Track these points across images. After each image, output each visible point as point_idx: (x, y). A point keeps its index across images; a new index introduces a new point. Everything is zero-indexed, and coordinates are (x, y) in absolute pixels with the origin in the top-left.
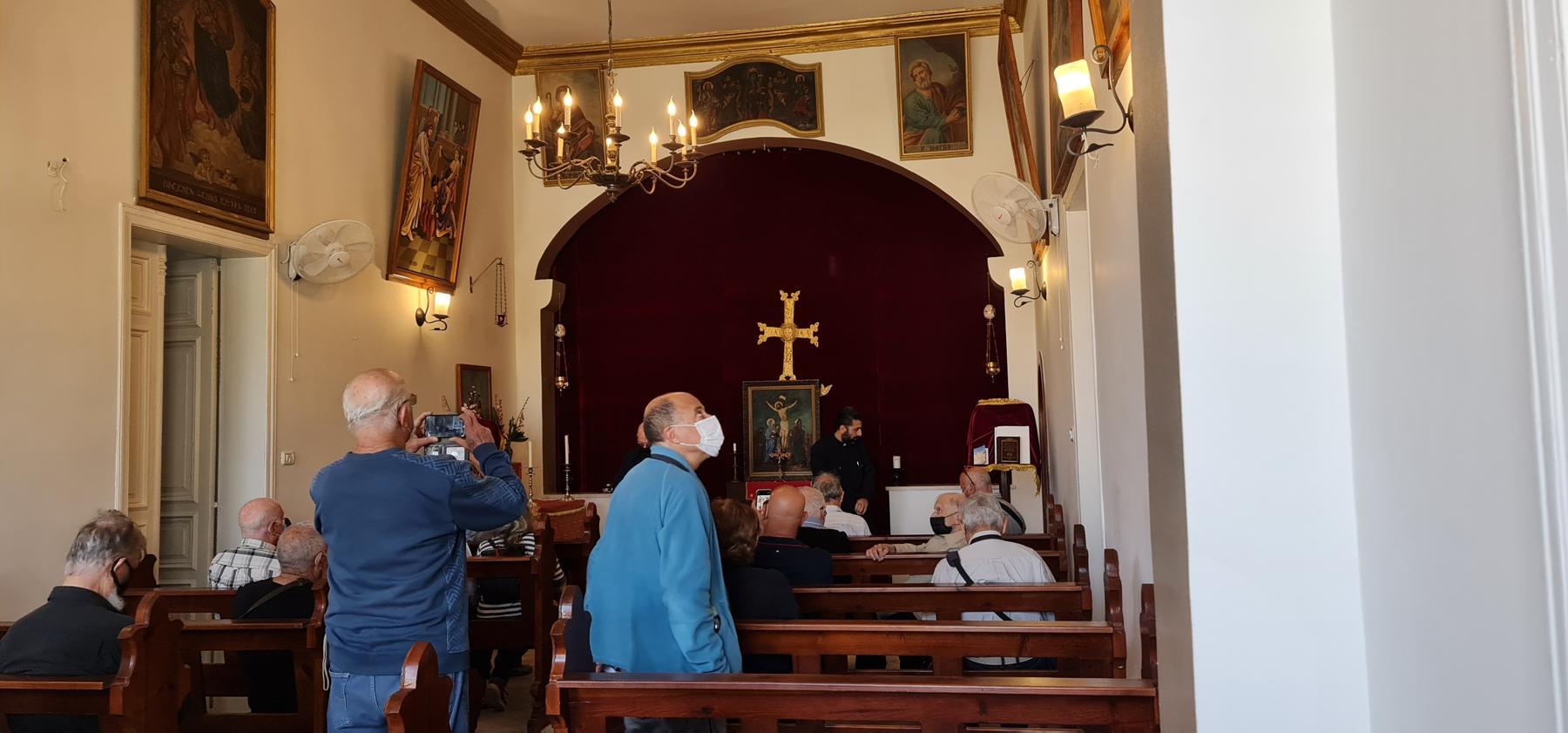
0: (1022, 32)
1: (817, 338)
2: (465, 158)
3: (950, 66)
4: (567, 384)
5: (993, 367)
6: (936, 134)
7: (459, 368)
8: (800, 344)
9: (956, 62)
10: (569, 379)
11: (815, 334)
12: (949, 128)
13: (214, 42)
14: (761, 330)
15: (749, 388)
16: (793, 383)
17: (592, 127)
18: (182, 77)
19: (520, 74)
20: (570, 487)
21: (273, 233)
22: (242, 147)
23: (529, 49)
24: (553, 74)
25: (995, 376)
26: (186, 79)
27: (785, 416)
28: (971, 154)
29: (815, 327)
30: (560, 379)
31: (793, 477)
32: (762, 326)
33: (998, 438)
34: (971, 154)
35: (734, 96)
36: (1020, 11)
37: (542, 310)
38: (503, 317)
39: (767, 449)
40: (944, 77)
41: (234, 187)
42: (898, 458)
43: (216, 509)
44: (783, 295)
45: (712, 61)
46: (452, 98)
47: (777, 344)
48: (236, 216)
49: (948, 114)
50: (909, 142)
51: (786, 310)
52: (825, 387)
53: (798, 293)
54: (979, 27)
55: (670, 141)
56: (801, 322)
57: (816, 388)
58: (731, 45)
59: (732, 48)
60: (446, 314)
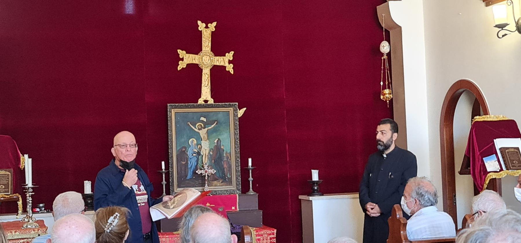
1: (232, 65)
14: (181, 57)
15: (172, 110)
16: (211, 106)
25: (389, 101)
27: (206, 136)
29: (230, 56)
31: (215, 191)
32: (182, 53)
39: (189, 167)
44: (201, 26)
53: (215, 24)
57: (234, 110)
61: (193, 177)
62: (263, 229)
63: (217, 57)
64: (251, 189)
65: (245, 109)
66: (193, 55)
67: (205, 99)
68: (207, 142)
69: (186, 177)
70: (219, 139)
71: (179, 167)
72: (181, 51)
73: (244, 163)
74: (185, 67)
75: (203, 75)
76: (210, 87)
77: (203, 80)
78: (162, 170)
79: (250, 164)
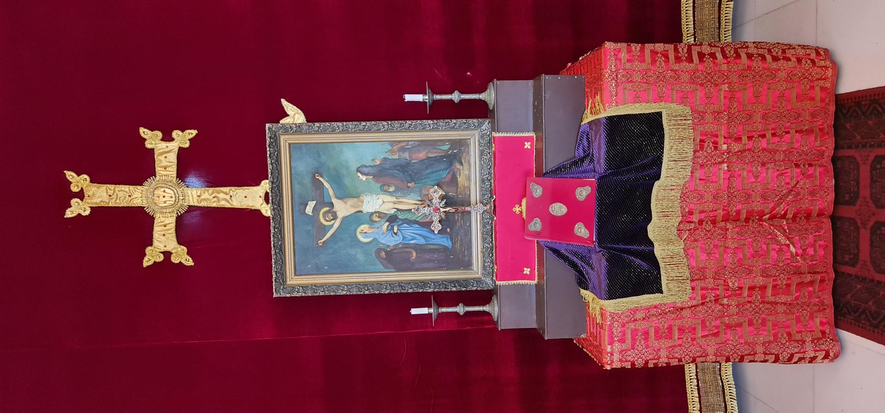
1: (176, 134)
11: (167, 138)
14: (161, 258)
15: (289, 282)
27: (351, 202)
29: (151, 138)
32: (151, 257)
39: (422, 241)
44: (77, 209)
52: (287, 115)
53: (70, 175)
61: (447, 232)
63: (158, 169)
65: (283, 101)
67: (261, 201)
68: (366, 199)
69: (446, 249)
70: (358, 170)
71: (426, 265)
72: (146, 259)
73: (417, 112)
74: (185, 248)
76: (233, 188)
77: (214, 205)
79: (419, 98)
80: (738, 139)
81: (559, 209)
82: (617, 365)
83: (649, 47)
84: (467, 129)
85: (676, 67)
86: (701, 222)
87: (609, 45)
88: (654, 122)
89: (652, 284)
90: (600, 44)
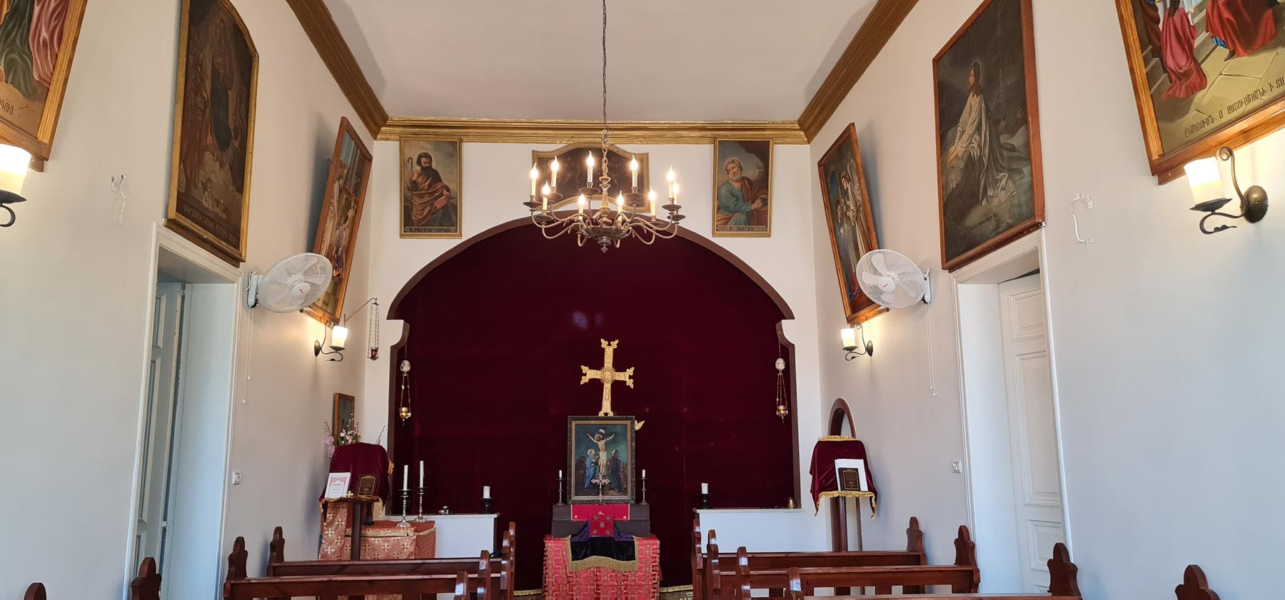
0: (809, 143)
2: (357, 208)
3: (757, 165)
4: (409, 414)
5: (783, 410)
6: (743, 217)
7: (337, 396)
8: (618, 386)
9: (763, 163)
10: (411, 410)
11: (630, 377)
12: (753, 213)
13: (222, 81)
16: (611, 419)
17: (448, 190)
18: (201, 110)
19: (382, 139)
20: (423, 509)
21: (245, 262)
22: (231, 180)
23: (394, 119)
24: (416, 142)
26: (204, 112)
27: (604, 447)
28: (769, 236)
29: (630, 371)
30: (404, 409)
31: (611, 500)
32: (585, 369)
33: (839, 469)
34: (769, 236)
35: (574, 173)
36: (813, 129)
37: (392, 347)
38: (376, 351)
39: (587, 475)
40: (752, 173)
41: (224, 216)
42: (707, 484)
43: (164, 530)
44: (604, 343)
45: (556, 143)
46: (357, 152)
47: (597, 385)
48: (224, 243)
49: (753, 203)
50: (720, 222)
51: (606, 356)
53: (617, 342)
54: (777, 137)
55: (669, 203)
56: (619, 366)
58: (574, 132)
59: (574, 134)
60: (342, 346)
62: (653, 539)
64: (644, 500)
66: (595, 371)
68: (605, 453)
75: (604, 390)
78: (559, 478)
79: (644, 475)
80: (625, 589)
81: (602, 525)
82: (546, 545)
83: (658, 556)
84: (632, 495)
85: (651, 566)
86: (596, 576)
87: (658, 542)
88: (632, 557)
89: (576, 556)
90: (659, 539)
